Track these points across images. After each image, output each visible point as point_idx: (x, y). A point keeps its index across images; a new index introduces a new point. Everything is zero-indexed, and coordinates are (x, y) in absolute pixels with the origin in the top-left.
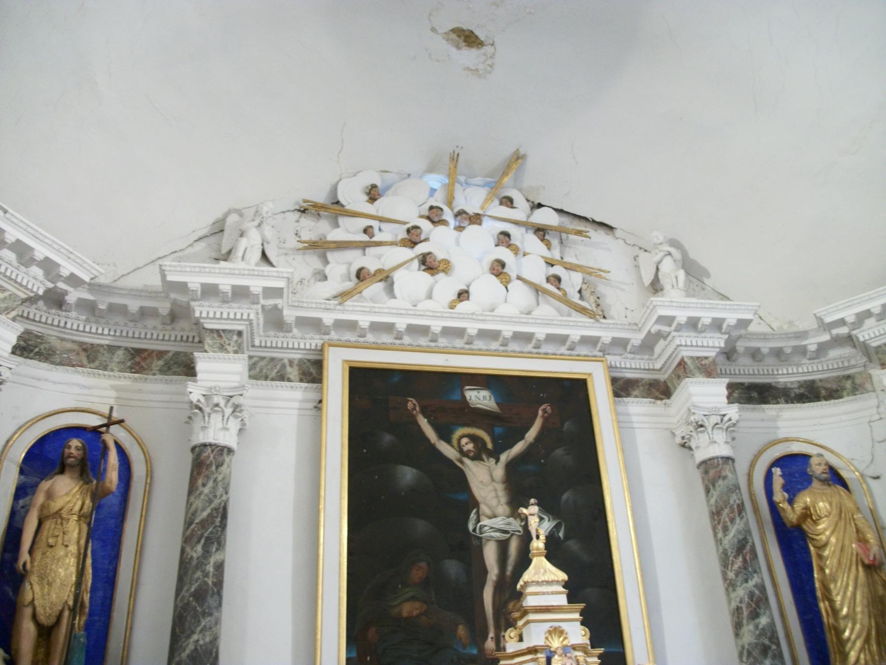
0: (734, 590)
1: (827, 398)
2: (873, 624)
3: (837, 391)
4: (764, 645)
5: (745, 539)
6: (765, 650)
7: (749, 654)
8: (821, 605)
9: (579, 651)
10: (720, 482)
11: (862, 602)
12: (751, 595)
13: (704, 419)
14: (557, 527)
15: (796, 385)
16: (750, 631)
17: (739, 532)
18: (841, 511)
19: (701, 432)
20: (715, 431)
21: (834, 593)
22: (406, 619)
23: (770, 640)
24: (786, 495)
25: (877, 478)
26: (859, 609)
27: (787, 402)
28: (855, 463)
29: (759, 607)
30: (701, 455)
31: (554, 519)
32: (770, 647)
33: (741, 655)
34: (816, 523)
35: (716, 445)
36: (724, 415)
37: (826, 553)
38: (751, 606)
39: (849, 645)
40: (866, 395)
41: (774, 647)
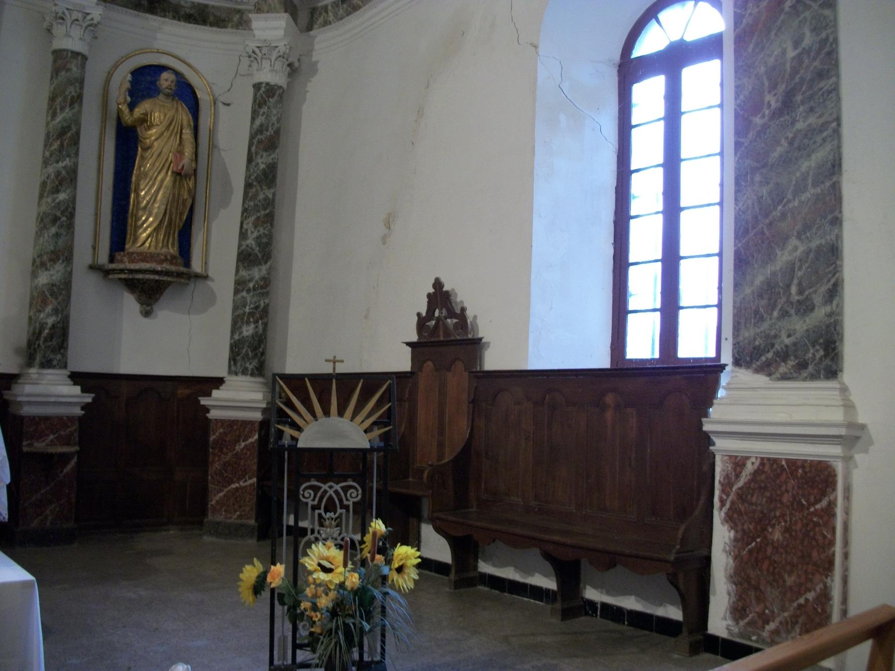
1: (212, 25)
3: (224, 21)
4: (56, 216)
5: (69, 128)
6: (55, 220)
10: (63, 73)
12: (58, 174)
13: (66, 12)
15: (188, 5)
17: (65, 120)
18: (170, 124)
19: (61, 24)
20: (73, 26)
21: (142, 187)
23: (63, 213)
24: (129, 99)
25: (229, 105)
27: (174, 18)
28: (214, 87)
29: (61, 184)
30: (58, 44)
32: (60, 219)
34: (150, 128)
35: (70, 40)
36: (88, 14)
37: (148, 154)
39: (141, 231)
40: (246, 32)
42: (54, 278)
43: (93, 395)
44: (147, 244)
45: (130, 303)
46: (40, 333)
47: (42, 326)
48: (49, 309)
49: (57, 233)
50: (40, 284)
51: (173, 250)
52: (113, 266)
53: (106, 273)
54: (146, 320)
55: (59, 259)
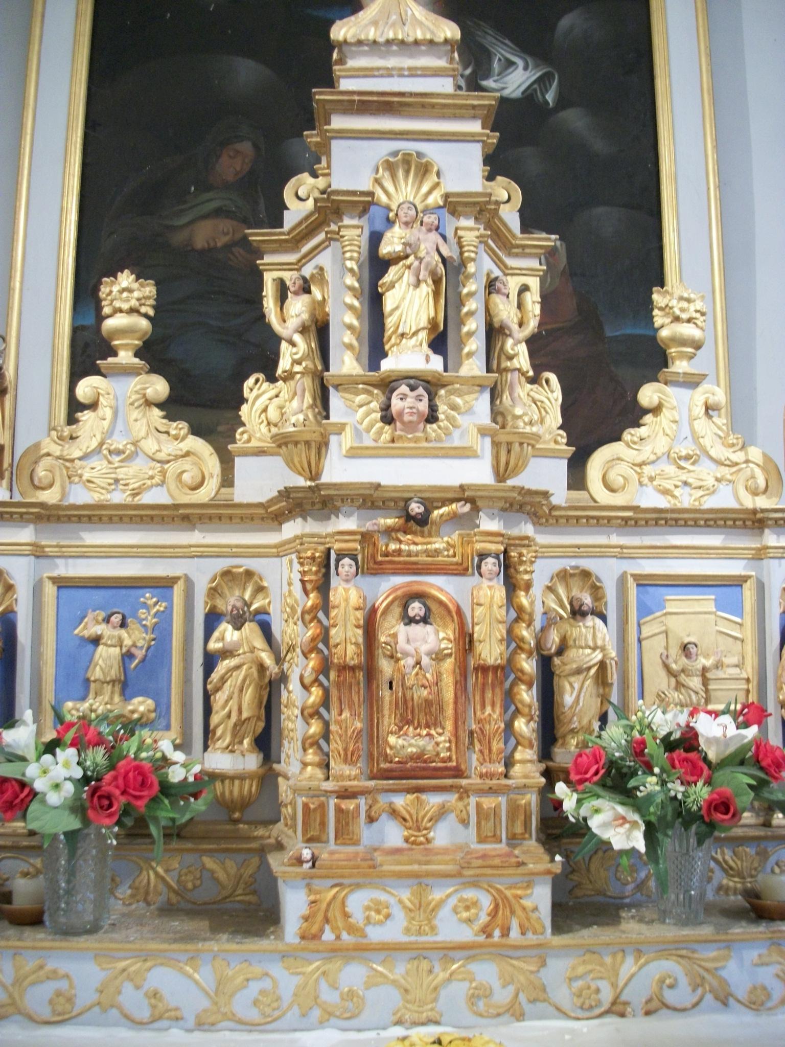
9: (467, 216)
14: (543, 81)
22: (202, 252)
31: (536, 66)
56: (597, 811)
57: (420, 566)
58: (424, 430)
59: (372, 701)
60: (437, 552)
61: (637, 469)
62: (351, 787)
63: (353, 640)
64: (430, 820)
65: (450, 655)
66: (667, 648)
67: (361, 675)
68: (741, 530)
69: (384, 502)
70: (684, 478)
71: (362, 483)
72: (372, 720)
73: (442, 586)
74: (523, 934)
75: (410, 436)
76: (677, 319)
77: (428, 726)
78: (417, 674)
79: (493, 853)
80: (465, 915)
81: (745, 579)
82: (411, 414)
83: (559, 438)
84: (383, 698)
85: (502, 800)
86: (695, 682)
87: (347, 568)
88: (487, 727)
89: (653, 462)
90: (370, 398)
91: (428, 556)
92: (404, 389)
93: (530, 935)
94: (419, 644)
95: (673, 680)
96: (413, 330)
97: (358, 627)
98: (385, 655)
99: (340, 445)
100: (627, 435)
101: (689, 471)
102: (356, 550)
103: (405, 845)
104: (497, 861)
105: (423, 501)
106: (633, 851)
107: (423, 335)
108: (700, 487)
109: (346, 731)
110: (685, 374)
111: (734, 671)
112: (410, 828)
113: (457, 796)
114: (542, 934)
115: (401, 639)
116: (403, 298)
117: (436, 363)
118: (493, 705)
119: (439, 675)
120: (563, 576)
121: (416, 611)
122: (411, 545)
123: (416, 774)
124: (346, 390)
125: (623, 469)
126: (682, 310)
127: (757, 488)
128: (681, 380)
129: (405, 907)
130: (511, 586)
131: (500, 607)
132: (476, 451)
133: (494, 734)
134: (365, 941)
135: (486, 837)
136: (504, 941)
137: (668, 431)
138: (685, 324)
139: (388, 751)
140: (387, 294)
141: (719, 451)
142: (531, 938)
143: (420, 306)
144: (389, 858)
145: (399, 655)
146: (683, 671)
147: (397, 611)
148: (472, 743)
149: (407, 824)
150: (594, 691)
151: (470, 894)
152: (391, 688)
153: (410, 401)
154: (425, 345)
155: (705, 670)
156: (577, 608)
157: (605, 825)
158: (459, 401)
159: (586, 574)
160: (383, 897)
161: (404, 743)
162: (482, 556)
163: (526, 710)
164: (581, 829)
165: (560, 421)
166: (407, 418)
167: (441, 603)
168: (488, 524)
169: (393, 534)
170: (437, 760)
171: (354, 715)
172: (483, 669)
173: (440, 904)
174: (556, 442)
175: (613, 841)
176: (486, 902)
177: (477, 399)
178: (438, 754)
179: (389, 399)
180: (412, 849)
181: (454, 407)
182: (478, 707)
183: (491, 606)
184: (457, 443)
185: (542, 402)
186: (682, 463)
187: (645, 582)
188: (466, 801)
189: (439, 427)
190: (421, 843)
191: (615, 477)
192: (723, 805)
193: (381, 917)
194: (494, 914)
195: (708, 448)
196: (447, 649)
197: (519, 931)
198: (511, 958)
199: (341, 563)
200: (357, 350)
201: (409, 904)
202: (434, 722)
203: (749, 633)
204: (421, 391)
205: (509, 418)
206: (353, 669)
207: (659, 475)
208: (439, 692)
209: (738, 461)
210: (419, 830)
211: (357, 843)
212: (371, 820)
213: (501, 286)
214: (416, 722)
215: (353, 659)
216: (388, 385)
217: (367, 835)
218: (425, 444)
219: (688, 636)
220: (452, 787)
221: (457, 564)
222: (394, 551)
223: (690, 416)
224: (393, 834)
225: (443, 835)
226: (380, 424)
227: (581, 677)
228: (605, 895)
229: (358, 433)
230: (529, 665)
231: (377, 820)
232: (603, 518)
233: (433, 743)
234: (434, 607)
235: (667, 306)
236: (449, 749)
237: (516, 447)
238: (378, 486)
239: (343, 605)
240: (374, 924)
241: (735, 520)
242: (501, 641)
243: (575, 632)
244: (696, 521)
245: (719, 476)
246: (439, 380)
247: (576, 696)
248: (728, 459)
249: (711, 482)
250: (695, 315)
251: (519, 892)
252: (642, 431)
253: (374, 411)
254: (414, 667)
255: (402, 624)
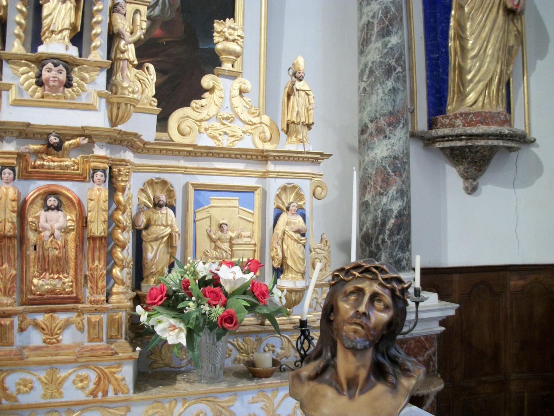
0: (368, 4)
2: (499, 70)
6: (389, 71)
7: (371, 72)
8: (451, 44)
11: (494, 46)
12: (386, 11)
16: (376, 48)
23: (397, 61)
26: (489, 52)
29: (391, 25)
32: (395, 70)
33: (362, 73)
38: (384, 23)
41: (399, 69)
42: (396, 148)
43: (457, 306)
44: (480, 104)
45: (452, 176)
46: (384, 223)
47: (386, 214)
48: (393, 191)
49: (394, 88)
50: (379, 157)
51: (501, 109)
52: (434, 133)
53: (427, 141)
54: (470, 198)
55: (399, 123)
56: (160, 322)
57: (56, 175)
58: (63, 92)
59: (22, 257)
60: (67, 167)
61: (198, 123)
62: (7, 310)
63: (10, 220)
64: (60, 329)
65: (73, 230)
66: (210, 226)
67: (16, 242)
68: (255, 161)
69: (34, 135)
70: (225, 130)
71: (17, 122)
72: (22, 269)
73: (70, 188)
74: (116, 394)
75: (54, 95)
76: (227, 39)
77: (58, 273)
78: (52, 241)
79: (98, 348)
80: (80, 385)
81: (256, 188)
82: (55, 81)
83: (153, 103)
84: (29, 256)
85: (104, 317)
86: (226, 246)
87: (7, 175)
88: (95, 273)
89: (208, 120)
90: (29, 70)
91: (61, 169)
92: (50, 65)
93: (120, 394)
94: (54, 223)
95: (213, 244)
96: (60, 29)
97: (13, 212)
98: (32, 230)
99: (8, 98)
100: (194, 103)
101: (228, 127)
102: (13, 164)
103: (44, 345)
104: (99, 353)
105: (58, 136)
106: (179, 345)
107: (66, 33)
108: (233, 136)
109: (5, 276)
110: (229, 70)
111: (247, 240)
112: (47, 334)
113: (76, 314)
114: (127, 393)
115: (42, 219)
116: (55, 9)
117: (73, 51)
118: (99, 260)
119: (66, 242)
120: (151, 183)
121: (52, 203)
122: (51, 162)
123: (51, 301)
124: (13, 63)
125: (190, 122)
126: (230, 34)
127: (265, 138)
128: (226, 74)
129: (42, 382)
130: (113, 189)
131: (104, 202)
132: (95, 107)
133: (100, 277)
134: (17, 404)
135: (93, 338)
136: (104, 398)
137: (217, 103)
138: (231, 43)
139: (33, 288)
140: (45, 5)
141: (245, 116)
142: (121, 396)
143: (65, 15)
144: (33, 353)
145: (41, 229)
146: (219, 239)
147: (40, 202)
148: (86, 283)
149: (45, 332)
150: (166, 251)
151: (84, 372)
152: (35, 249)
153: (54, 73)
154: (67, 40)
155: (231, 239)
156: (157, 202)
157: (164, 330)
158: (87, 75)
159: (164, 183)
160: (28, 377)
161: (41, 283)
162: (95, 170)
163: (120, 263)
164: (151, 332)
165: (154, 92)
166: (51, 83)
167: (68, 198)
168: (99, 151)
169: (39, 155)
170: (64, 293)
171: (10, 266)
172: (94, 239)
173: (65, 378)
174: (151, 105)
175: (168, 339)
176: (93, 376)
177: (98, 75)
178: (64, 289)
179: (41, 71)
180: (47, 347)
181: (83, 79)
182: (90, 261)
183: (99, 201)
184: (84, 101)
185: (144, 80)
186: (224, 122)
187: (199, 188)
188: (82, 317)
189: (73, 91)
190: (54, 343)
191: (185, 127)
192: (229, 319)
193: (27, 389)
194: (98, 383)
195: (240, 114)
196: (71, 226)
197: (113, 392)
198: (109, 408)
199: (3, 171)
200: (23, 39)
201: (45, 380)
202: (62, 270)
203: (256, 219)
204: (61, 67)
205: (119, 88)
206: (10, 238)
207: (211, 127)
208: (66, 252)
209: (256, 122)
210: (52, 335)
211: (12, 344)
212: (22, 330)
213: (120, 8)
214: (50, 271)
215: (9, 231)
216: (41, 62)
217: (18, 339)
218: (64, 101)
219: (223, 219)
220: (73, 308)
221: (79, 174)
222: (39, 165)
223: (230, 95)
224: (36, 338)
225: (67, 338)
226: (34, 86)
227: (158, 242)
228: (170, 366)
229: (20, 91)
230: (126, 237)
231: (25, 330)
232: (176, 150)
233: (61, 283)
234: (64, 201)
235: (222, 31)
236: (72, 286)
237: (123, 106)
238: (28, 125)
239: (4, 197)
240: (23, 393)
241: (252, 155)
242: (104, 222)
243: (155, 217)
244: (230, 155)
245: (245, 130)
246: (74, 61)
247: (154, 253)
248: (251, 121)
249: (240, 133)
250: (237, 38)
251: (114, 370)
252: (203, 102)
253: (32, 78)
254: (50, 237)
255: (43, 211)
